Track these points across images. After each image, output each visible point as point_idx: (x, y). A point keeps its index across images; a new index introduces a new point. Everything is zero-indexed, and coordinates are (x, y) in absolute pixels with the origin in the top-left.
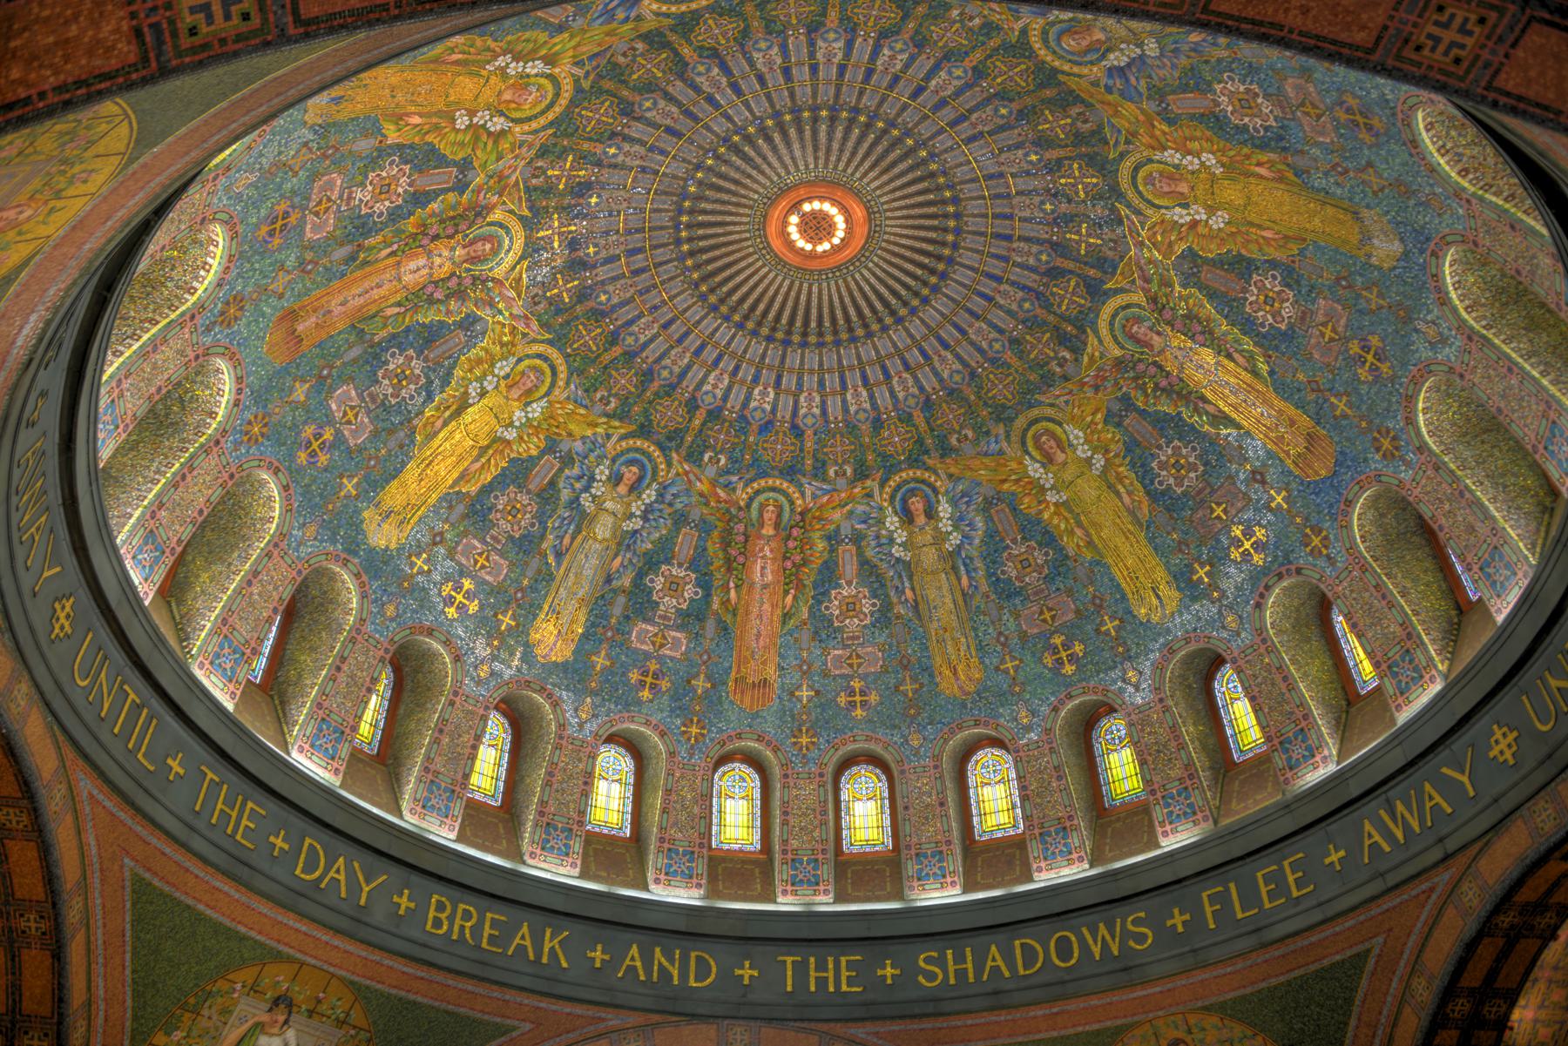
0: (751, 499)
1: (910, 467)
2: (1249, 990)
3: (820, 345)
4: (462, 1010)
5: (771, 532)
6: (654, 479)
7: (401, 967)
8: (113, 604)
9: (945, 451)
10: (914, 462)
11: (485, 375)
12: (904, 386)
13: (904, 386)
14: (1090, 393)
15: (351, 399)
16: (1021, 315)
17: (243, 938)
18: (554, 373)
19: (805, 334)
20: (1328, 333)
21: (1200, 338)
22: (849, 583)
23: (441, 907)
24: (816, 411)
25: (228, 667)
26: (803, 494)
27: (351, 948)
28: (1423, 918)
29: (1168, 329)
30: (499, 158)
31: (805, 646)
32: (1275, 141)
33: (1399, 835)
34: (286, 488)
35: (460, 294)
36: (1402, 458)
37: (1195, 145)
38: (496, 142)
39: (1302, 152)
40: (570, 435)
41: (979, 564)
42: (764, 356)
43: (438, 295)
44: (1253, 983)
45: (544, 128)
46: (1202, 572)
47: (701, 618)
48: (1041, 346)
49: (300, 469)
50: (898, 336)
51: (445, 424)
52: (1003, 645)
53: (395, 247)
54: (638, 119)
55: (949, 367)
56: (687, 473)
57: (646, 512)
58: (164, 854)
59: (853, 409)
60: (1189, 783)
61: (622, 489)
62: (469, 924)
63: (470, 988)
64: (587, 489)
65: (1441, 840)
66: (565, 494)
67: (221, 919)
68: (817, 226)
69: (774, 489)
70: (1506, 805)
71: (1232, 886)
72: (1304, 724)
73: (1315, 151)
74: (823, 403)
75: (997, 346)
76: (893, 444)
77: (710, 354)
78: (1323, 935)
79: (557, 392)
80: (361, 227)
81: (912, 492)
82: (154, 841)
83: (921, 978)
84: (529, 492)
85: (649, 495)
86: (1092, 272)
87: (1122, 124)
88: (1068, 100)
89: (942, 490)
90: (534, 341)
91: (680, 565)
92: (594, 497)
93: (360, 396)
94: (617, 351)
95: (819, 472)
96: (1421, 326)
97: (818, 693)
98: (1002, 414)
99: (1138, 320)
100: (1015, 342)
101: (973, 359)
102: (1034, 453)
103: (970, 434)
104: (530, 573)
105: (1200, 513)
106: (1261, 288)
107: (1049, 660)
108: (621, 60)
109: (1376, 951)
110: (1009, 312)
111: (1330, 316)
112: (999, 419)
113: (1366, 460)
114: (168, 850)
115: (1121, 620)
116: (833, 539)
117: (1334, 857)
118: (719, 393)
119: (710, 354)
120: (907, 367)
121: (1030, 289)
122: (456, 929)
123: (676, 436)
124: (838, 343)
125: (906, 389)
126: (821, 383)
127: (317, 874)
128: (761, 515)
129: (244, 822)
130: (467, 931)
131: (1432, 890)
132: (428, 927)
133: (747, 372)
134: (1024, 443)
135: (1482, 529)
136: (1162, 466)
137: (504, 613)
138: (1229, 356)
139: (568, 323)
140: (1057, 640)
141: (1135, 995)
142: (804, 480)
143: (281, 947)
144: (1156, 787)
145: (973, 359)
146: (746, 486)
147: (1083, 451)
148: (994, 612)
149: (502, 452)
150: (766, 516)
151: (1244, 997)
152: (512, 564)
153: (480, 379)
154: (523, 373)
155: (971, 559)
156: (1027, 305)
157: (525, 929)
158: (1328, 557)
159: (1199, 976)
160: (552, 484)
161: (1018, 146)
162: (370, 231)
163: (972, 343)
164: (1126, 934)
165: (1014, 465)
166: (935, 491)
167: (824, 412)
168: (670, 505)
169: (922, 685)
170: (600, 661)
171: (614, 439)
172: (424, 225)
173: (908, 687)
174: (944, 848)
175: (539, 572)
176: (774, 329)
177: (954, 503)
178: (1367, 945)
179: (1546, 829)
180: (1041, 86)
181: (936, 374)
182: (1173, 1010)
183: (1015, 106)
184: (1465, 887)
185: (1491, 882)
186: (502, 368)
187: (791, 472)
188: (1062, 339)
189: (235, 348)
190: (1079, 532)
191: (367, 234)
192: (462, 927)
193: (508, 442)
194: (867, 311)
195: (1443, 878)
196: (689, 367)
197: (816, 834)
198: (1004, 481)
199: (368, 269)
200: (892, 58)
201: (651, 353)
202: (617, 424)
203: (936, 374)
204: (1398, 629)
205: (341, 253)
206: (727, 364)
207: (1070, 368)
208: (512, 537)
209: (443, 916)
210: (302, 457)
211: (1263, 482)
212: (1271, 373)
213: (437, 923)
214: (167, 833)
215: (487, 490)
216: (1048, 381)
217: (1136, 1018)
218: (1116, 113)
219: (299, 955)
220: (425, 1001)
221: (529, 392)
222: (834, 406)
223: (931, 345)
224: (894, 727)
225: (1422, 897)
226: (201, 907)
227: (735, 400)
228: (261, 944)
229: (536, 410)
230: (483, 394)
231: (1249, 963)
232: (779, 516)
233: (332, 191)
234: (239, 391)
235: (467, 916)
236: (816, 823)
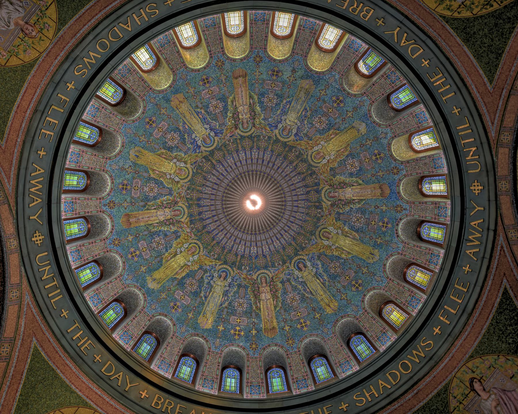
0: (257, 277)
1: (296, 256)
2: (480, 338)
3: (264, 232)
5: (265, 285)
6: (230, 276)
8: (57, 246)
9: (303, 249)
10: (296, 255)
11: (181, 247)
12: (287, 236)
13: (287, 236)
14: (329, 216)
16: (306, 207)
17: (73, 392)
18: (199, 248)
19: (259, 231)
20: (367, 160)
21: (345, 187)
22: (290, 293)
24: (268, 250)
25: (95, 302)
27: (118, 407)
28: (510, 260)
29: (337, 190)
30: (179, 189)
31: (283, 314)
32: (330, 126)
33: (477, 243)
34: (124, 262)
35: (173, 224)
36: (401, 170)
37: (318, 142)
38: (177, 184)
39: (336, 123)
40: (206, 264)
41: (323, 273)
42: (251, 239)
43: (167, 223)
44: (479, 333)
45: (187, 182)
46: (379, 241)
47: (251, 313)
48: (314, 212)
49: (129, 259)
50: (281, 224)
51: (171, 258)
52: (340, 292)
54: (208, 181)
55: (295, 227)
56: (239, 273)
57: (229, 285)
58: (49, 341)
59: (276, 247)
60: (412, 294)
61: (222, 279)
64: (212, 279)
65: (488, 229)
66: (206, 281)
67: (66, 380)
68: (254, 203)
69: (263, 273)
70: (493, 198)
71: (445, 307)
72: (431, 252)
73: (337, 120)
74: (269, 247)
75: (304, 217)
76: (289, 252)
77: (238, 241)
78: (486, 295)
79: (201, 253)
80: (146, 199)
81: (299, 263)
82: (47, 334)
83: (357, 404)
84: (196, 280)
85: (229, 280)
86: (315, 188)
87: (303, 147)
88: (291, 148)
89: (306, 259)
90: (193, 239)
91: (241, 299)
92: (214, 281)
93: (147, 245)
94: (215, 242)
95: (273, 266)
96: (381, 136)
97: (291, 327)
98: (312, 233)
99: (330, 192)
100: (307, 214)
101: (300, 223)
102: (324, 239)
103: (307, 242)
104: (197, 302)
105: (370, 227)
106: (349, 164)
107: (354, 289)
108: (201, 164)
109: (508, 287)
110: (303, 208)
111: (365, 157)
112: (312, 235)
113: (394, 179)
114: (51, 340)
115: (367, 267)
116: (283, 282)
117: (467, 269)
118: (243, 251)
119: (238, 241)
120: (286, 231)
121: (305, 199)
122: (164, 408)
123: (234, 263)
124: (267, 231)
125: (287, 237)
126: (267, 242)
128: (261, 281)
131: (502, 247)
133: (248, 244)
134: (320, 238)
135: (427, 161)
136: (354, 222)
137: (190, 313)
138: (353, 185)
139: (201, 235)
140: (354, 283)
141: (441, 367)
143: (88, 400)
144: (404, 302)
145: (300, 223)
147: (335, 232)
148: (333, 284)
150: (263, 281)
151: (481, 342)
152: (192, 299)
153: (180, 248)
154: (191, 248)
155: (321, 273)
156: (306, 204)
158: (404, 209)
159: (458, 343)
160: (202, 278)
161: (287, 166)
163: (298, 219)
164: (423, 348)
165: (321, 244)
166: (304, 260)
167: (270, 250)
169: (321, 314)
170: (221, 328)
171: (218, 265)
172: (162, 203)
173: (318, 316)
174: (348, 359)
175: (200, 302)
176: (252, 231)
177: (310, 261)
178: (503, 287)
179: (508, 187)
180: (285, 148)
181: (293, 230)
182: (460, 365)
183: (282, 156)
184: (510, 235)
185: (513, 223)
186: (186, 245)
187: (266, 267)
188: (317, 207)
189: (112, 216)
190: (344, 252)
191: (148, 201)
193: (189, 266)
194: (272, 221)
195: (501, 239)
196: (233, 245)
197: (302, 371)
198: (320, 250)
199: (149, 211)
200: (255, 154)
201: (223, 242)
202: (218, 261)
203: (293, 230)
204: (432, 206)
205: (142, 204)
206: (243, 242)
207: (322, 213)
208: (191, 292)
209: (160, 402)
210: (130, 256)
211: (378, 207)
212: (363, 181)
214: (53, 332)
215: (183, 278)
216: (319, 219)
217: (449, 378)
218: (301, 146)
219: (95, 406)
221: (193, 253)
222: (272, 248)
223: (289, 224)
224: (318, 329)
225: (502, 252)
226: (58, 371)
227: (247, 252)
228: (80, 397)
229: (196, 257)
230: (181, 252)
231: (471, 325)
232: (266, 280)
234: (112, 229)
236: (302, 367)
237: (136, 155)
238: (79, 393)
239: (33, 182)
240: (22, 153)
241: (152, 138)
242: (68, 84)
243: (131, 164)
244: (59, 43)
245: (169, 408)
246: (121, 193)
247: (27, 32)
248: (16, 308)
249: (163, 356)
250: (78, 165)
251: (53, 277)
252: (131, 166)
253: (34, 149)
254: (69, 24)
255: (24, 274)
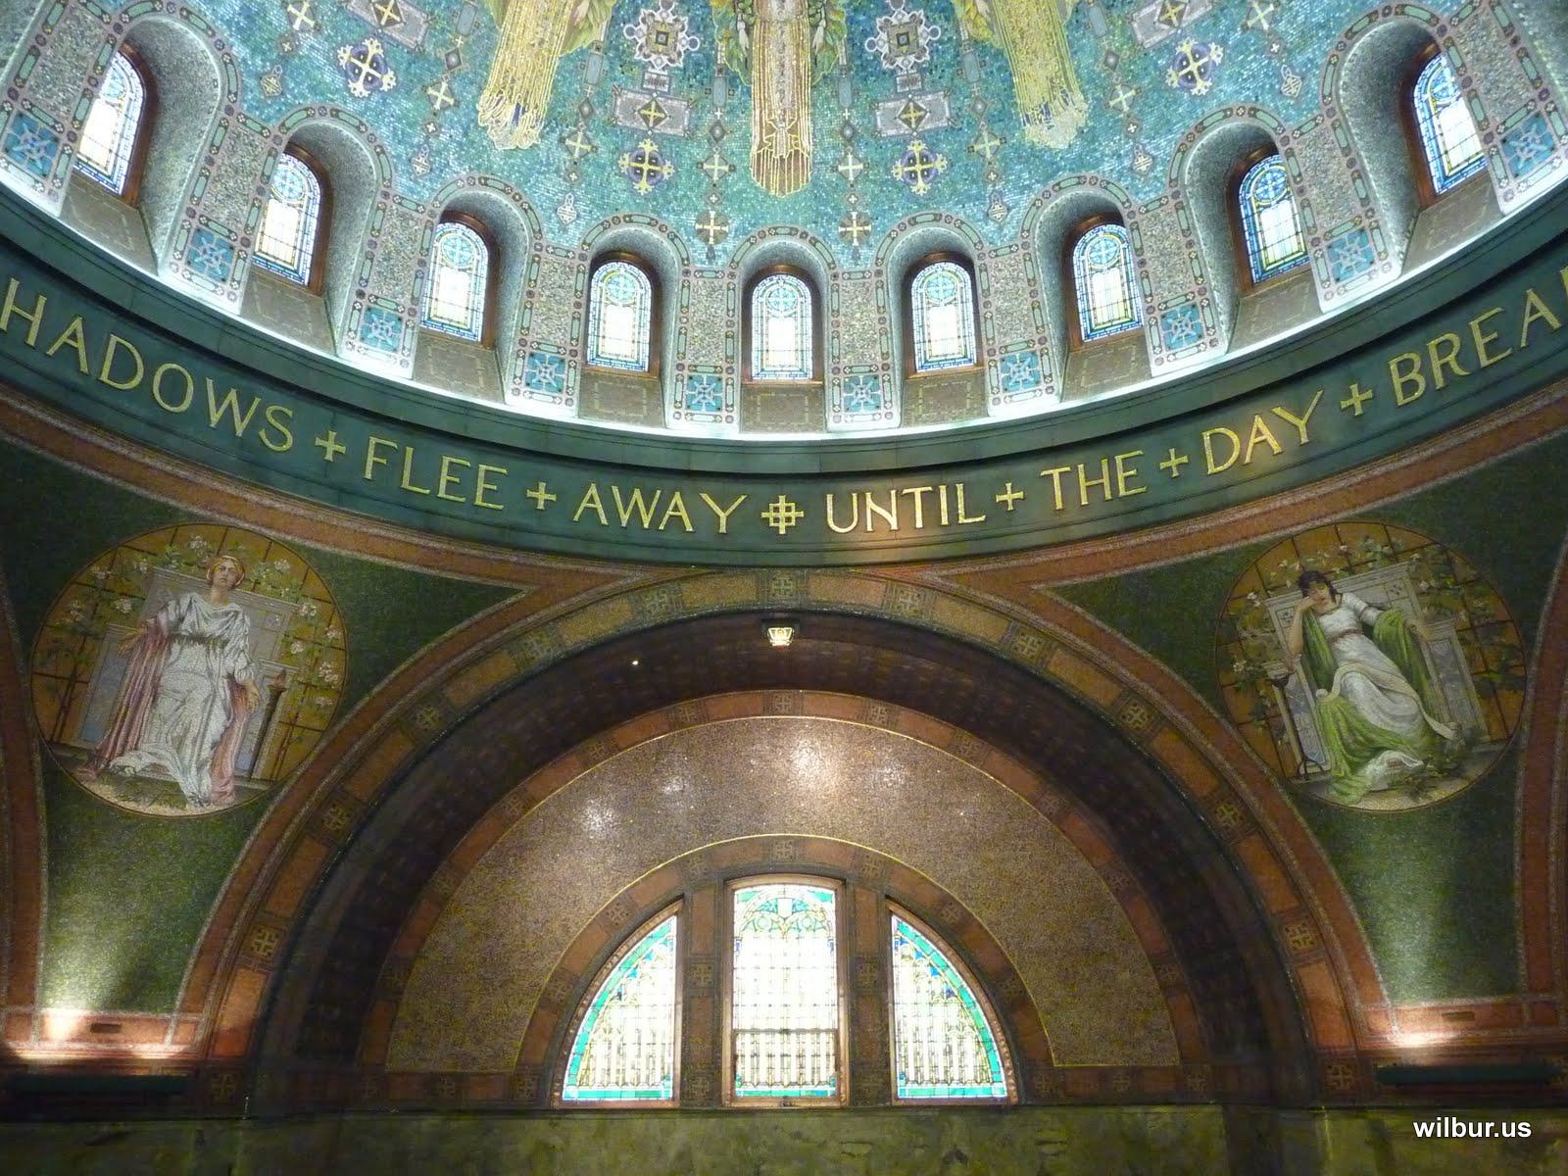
4: (1520, 449)
7: (1398, 465)
15: (895, 109)
23: (1405, 367)
25: (1026, 375)
27: (1325, 489)
53: (741, 26)
62: (1451, 358)
63: (1500, 422)
93: (898, 96)
114: (1057, 556)
127: (1235, 455)
129: (1121, 476)
130: (1454, 365)
132: (1401, 401)
157: (1533, 298)
162: (707, 57)
191: (710, 60)
192: (1445, 367)
205: (719, 87)
209: (1413, 375)
213: (1409, 387)
220: (1462, 473)
226: (1142, 567)
233: (638, 103)
235: (1444, 348)
237: (516, 117)
238: (1223, 549)
239: (625, 518)
240: (547, 552)
241: (429, 48)
242: (329, 457)
243: (555, 136)
244: (225, 509)
245: (1451, 358)
246: (669, 183)
247: (231, 578)
248: (945, 604)
249: (1319, 234)
250: (567, 358)
251: (899, 495)
252: (562, 140)
253: (532, 523)
254: (163, 499)
255: (867, 571)
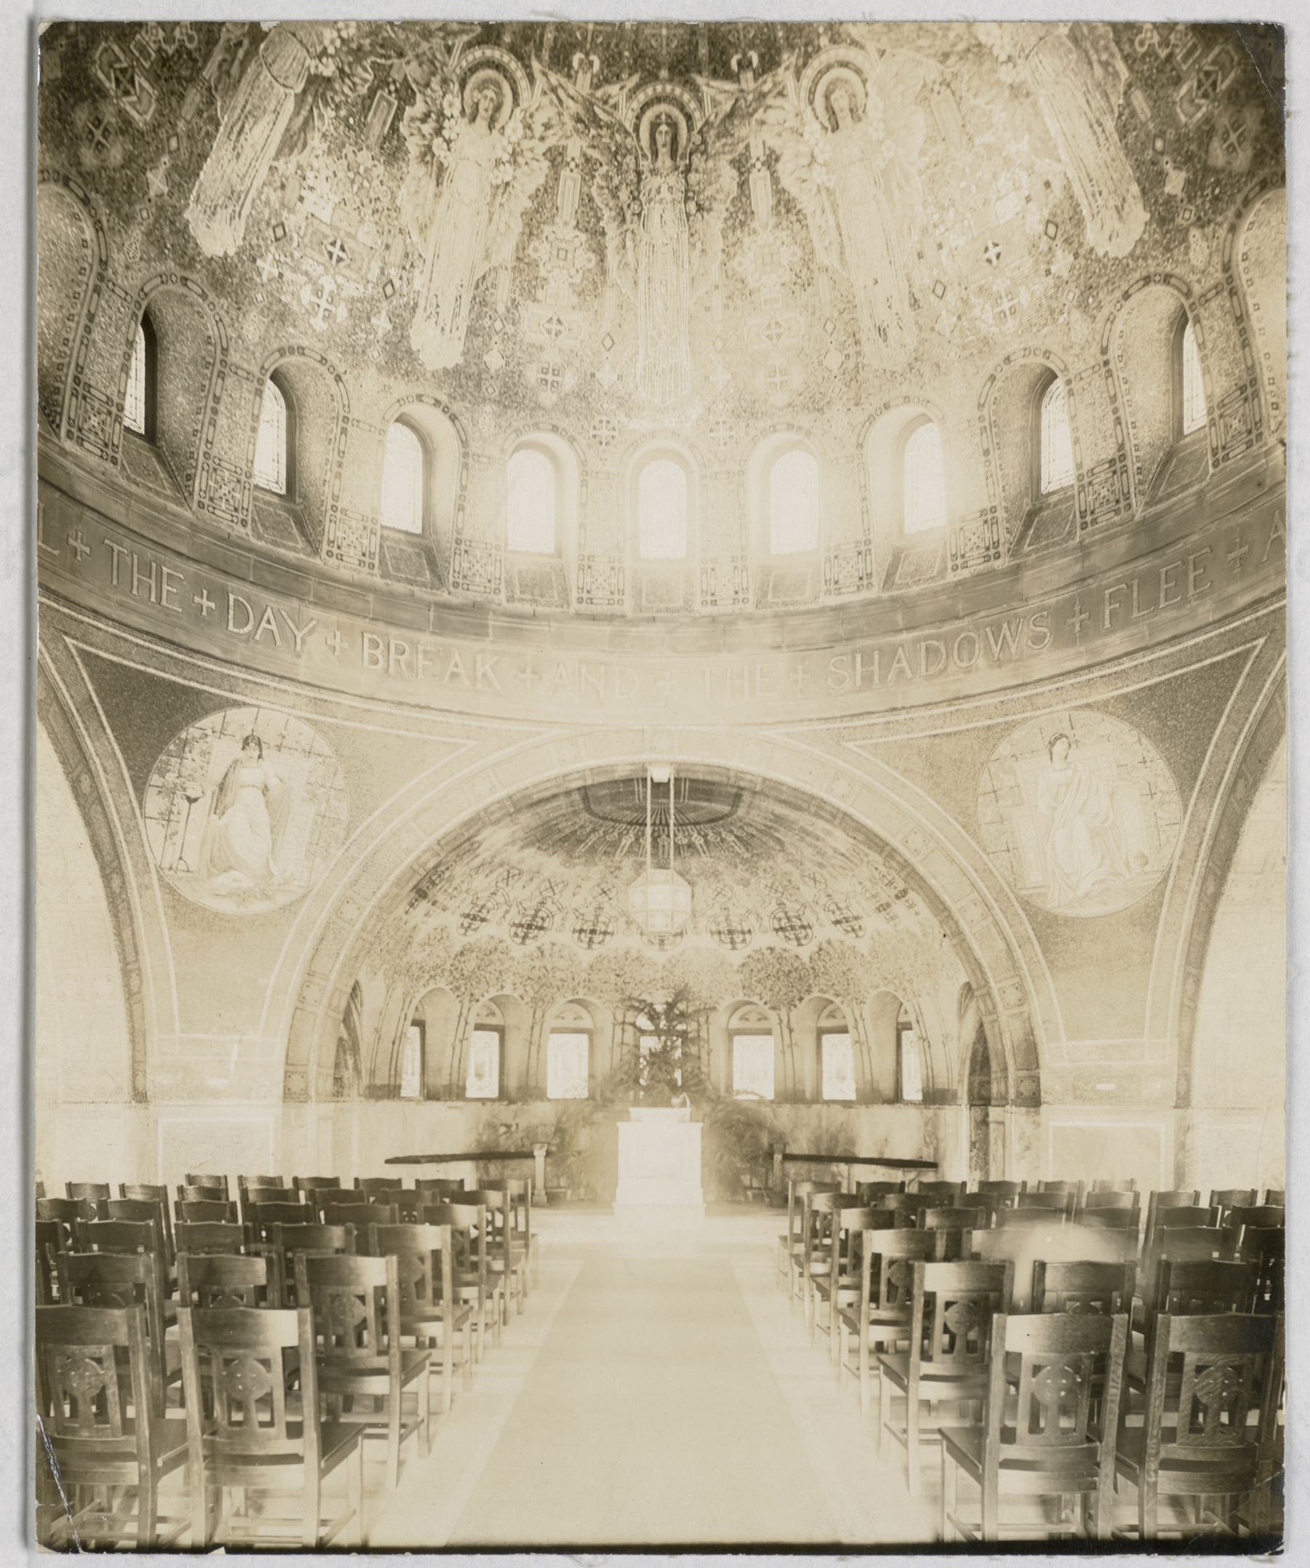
26: (700, 101)
57: (514, 154)
92: (448, 142)
142: (700, 80)
146: (629, 98)
149: (323, 96)
168: (542, 139)
171: (456, 52)
193: (329, 80)
232: (675, 140)
